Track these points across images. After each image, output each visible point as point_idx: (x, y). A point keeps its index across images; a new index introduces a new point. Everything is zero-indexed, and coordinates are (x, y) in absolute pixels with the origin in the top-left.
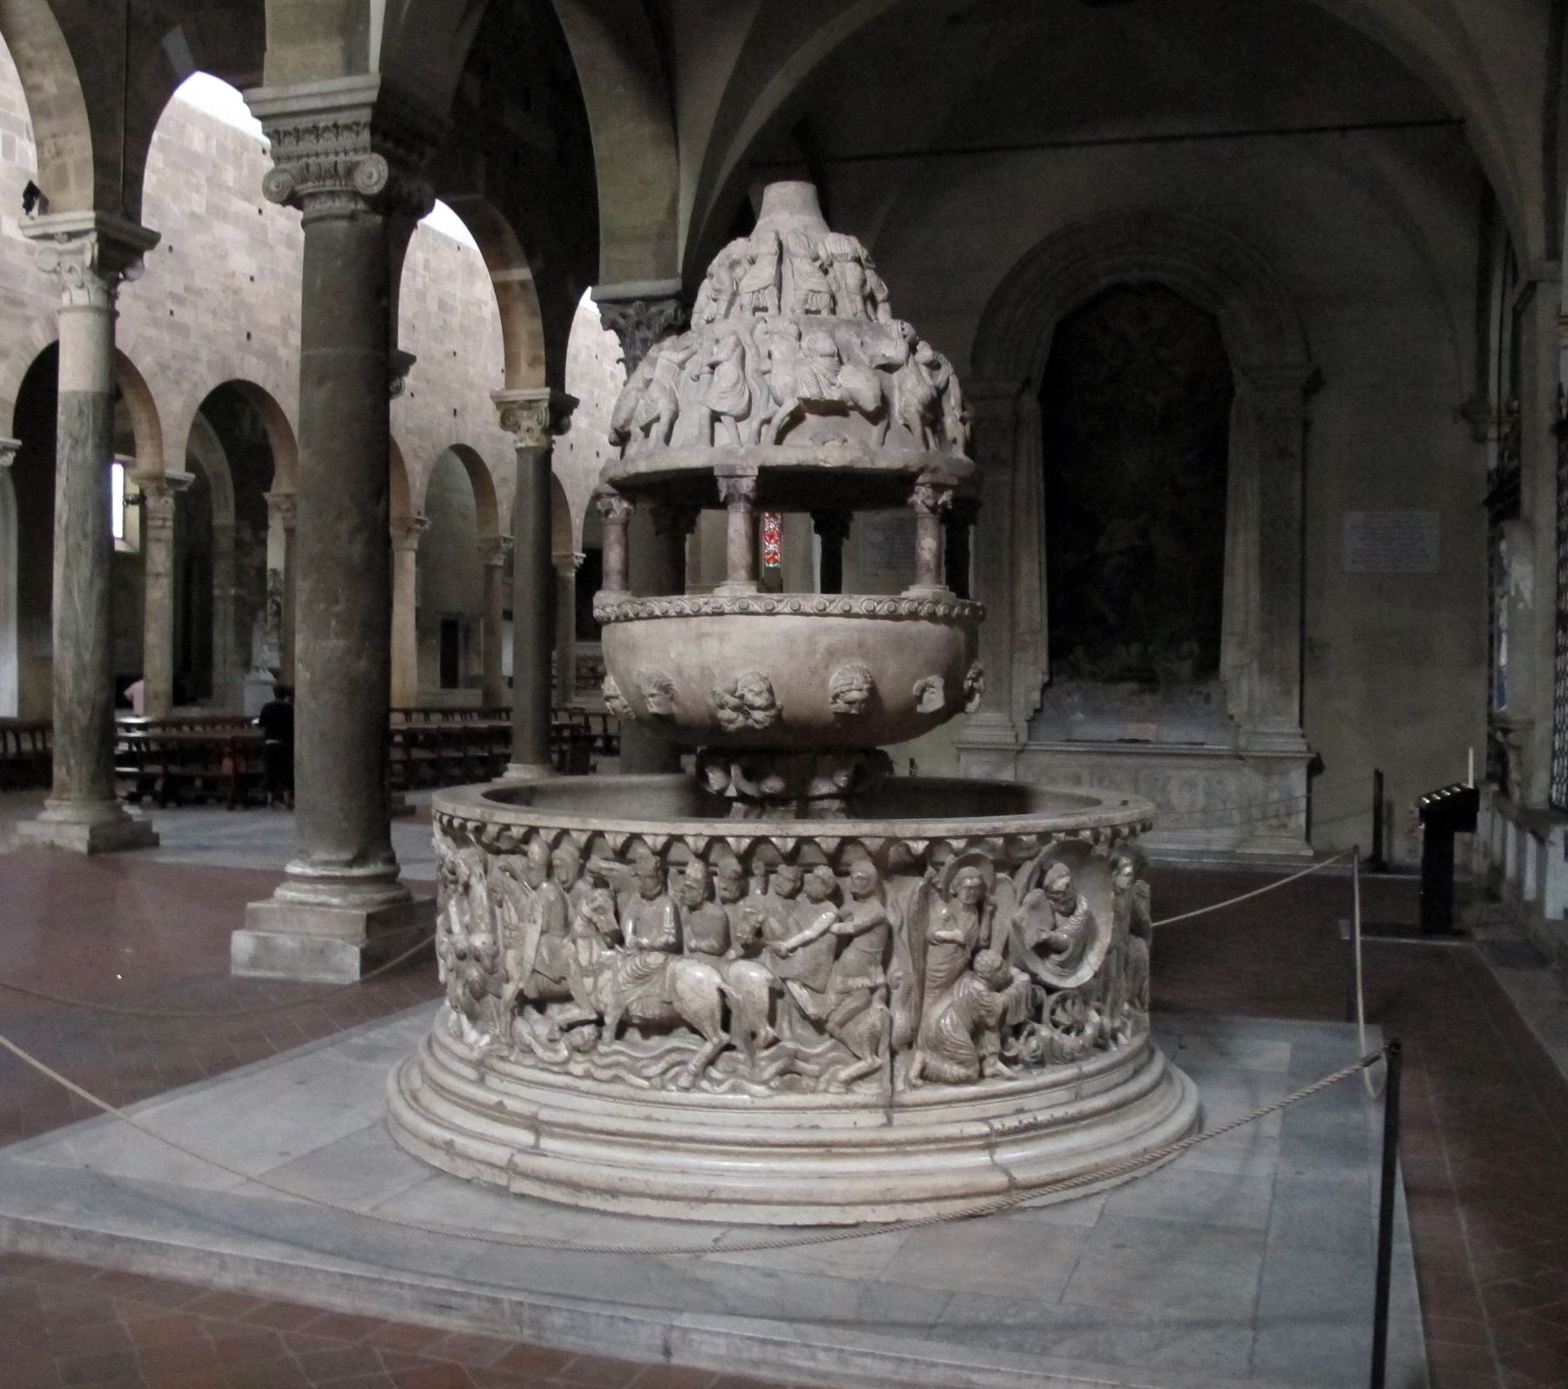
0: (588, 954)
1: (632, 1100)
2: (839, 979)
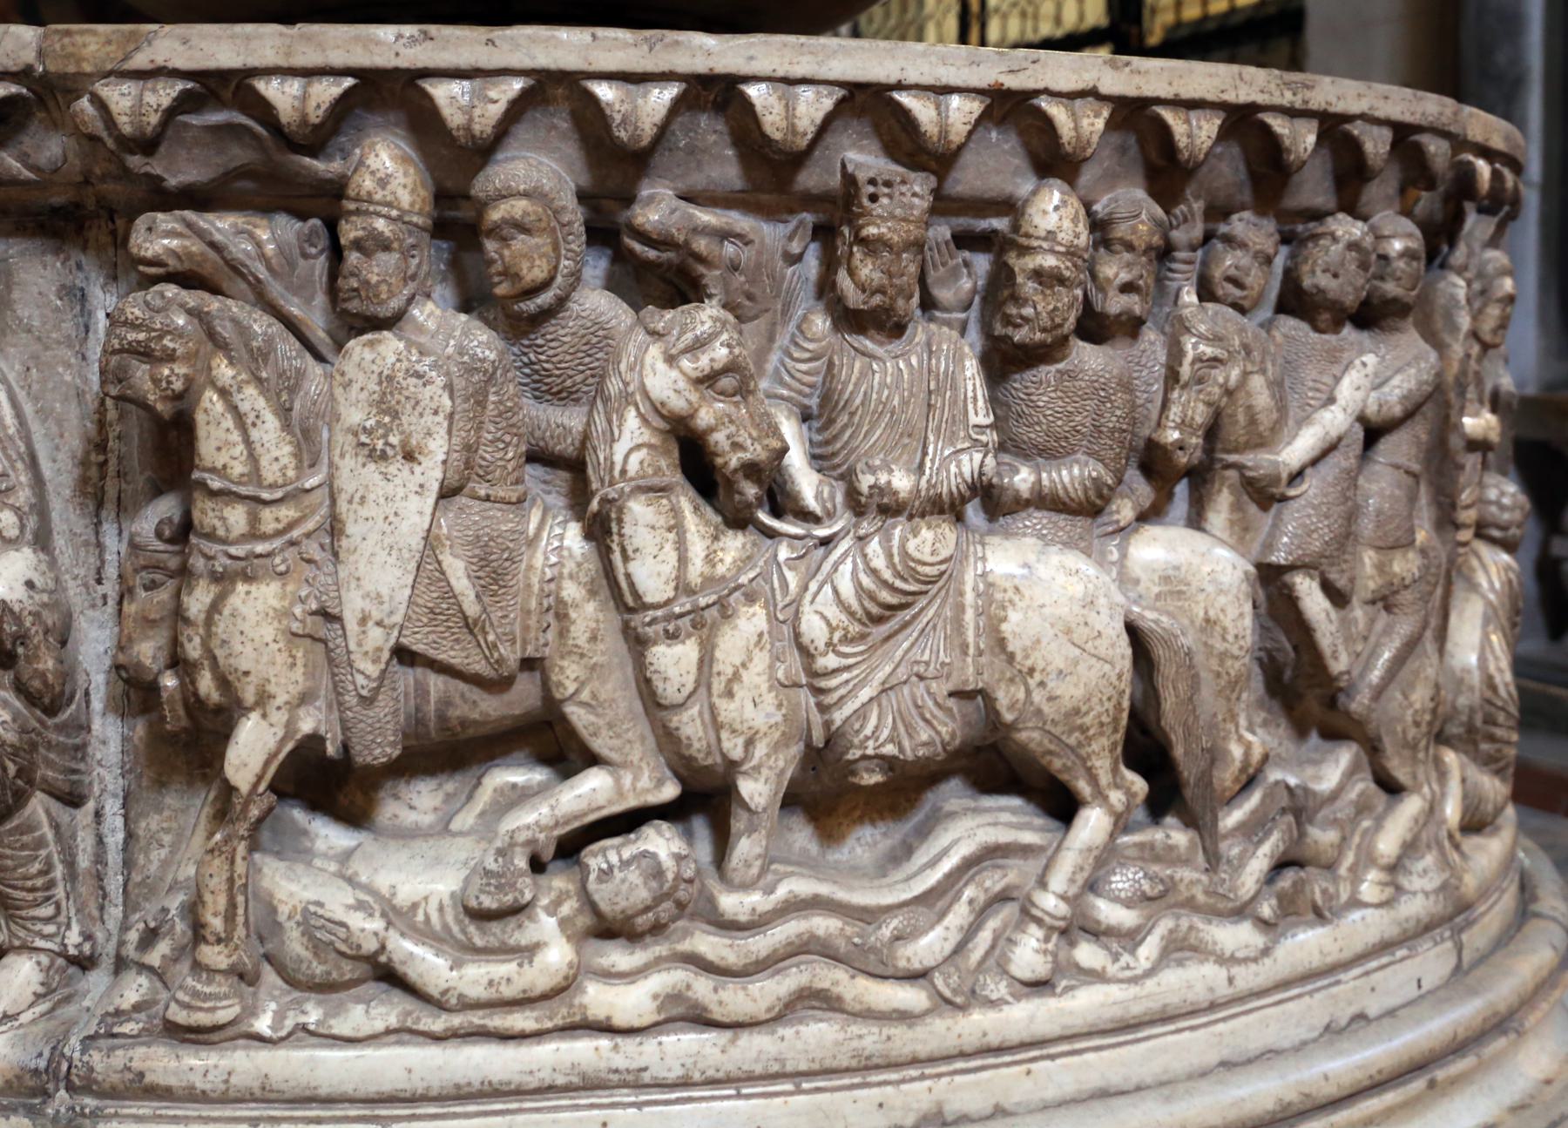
0: (671, 556)
1: (866, 1067)
2: (1369, 558)
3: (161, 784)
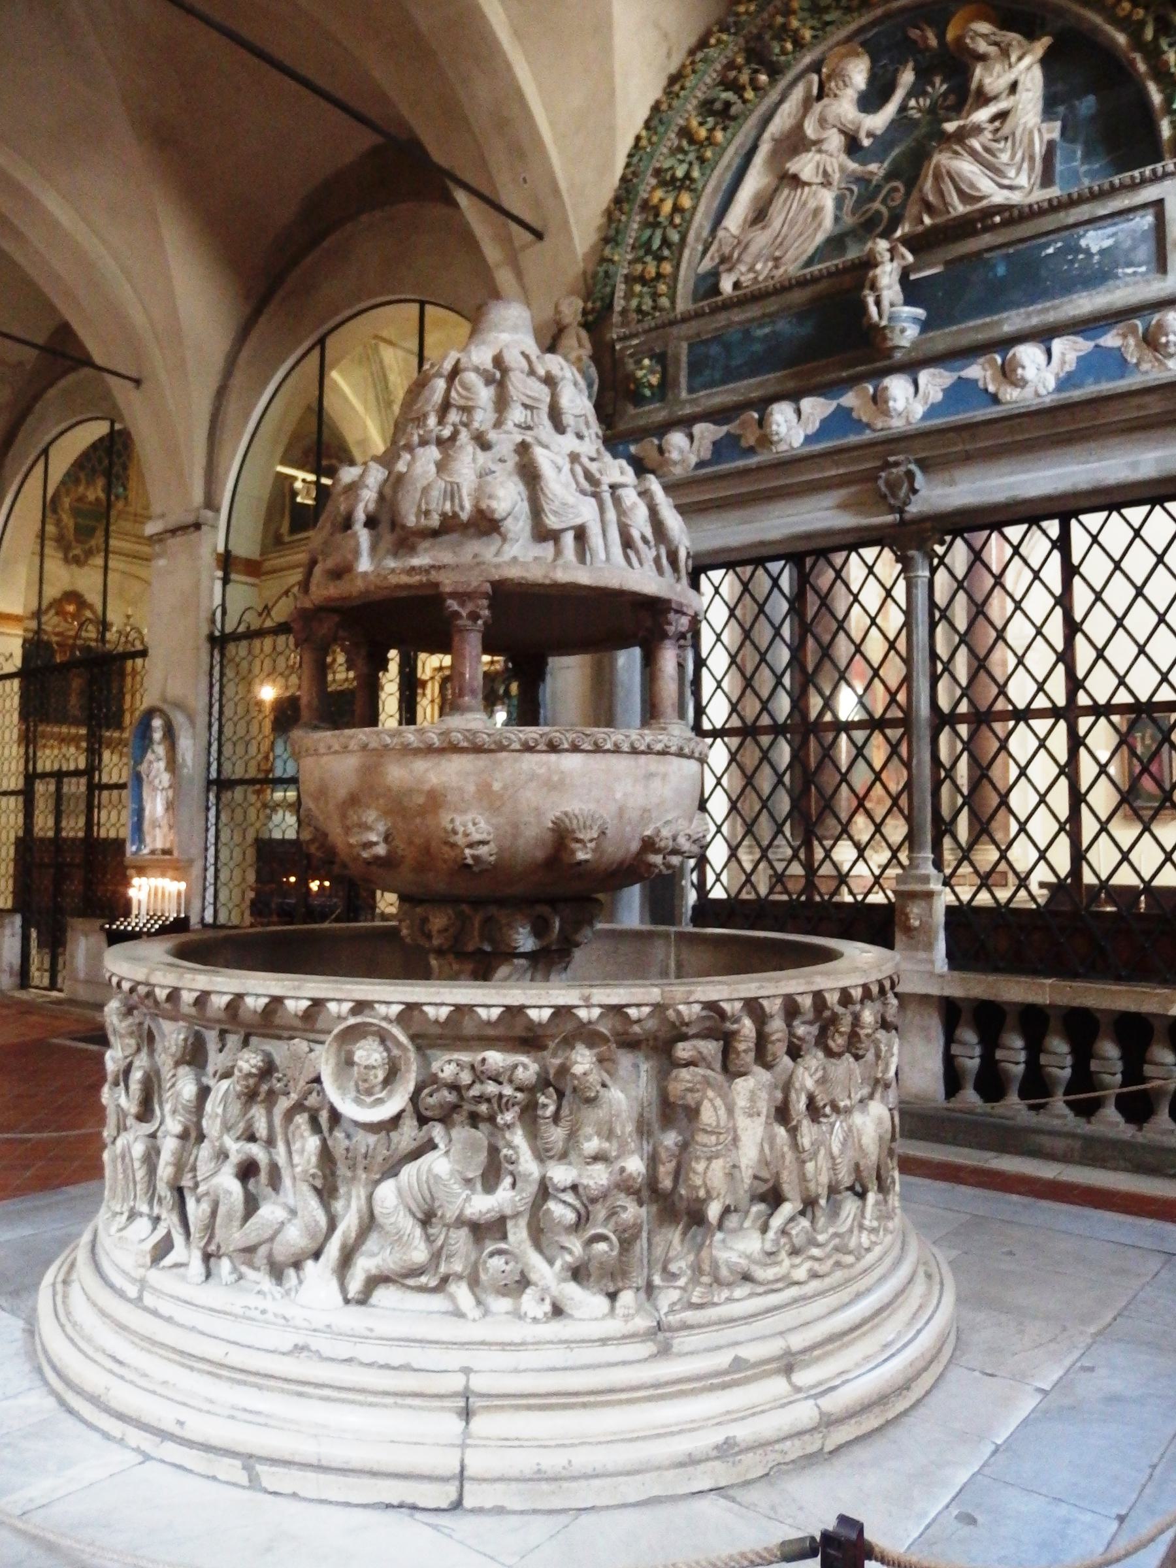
3: (661, 1225)
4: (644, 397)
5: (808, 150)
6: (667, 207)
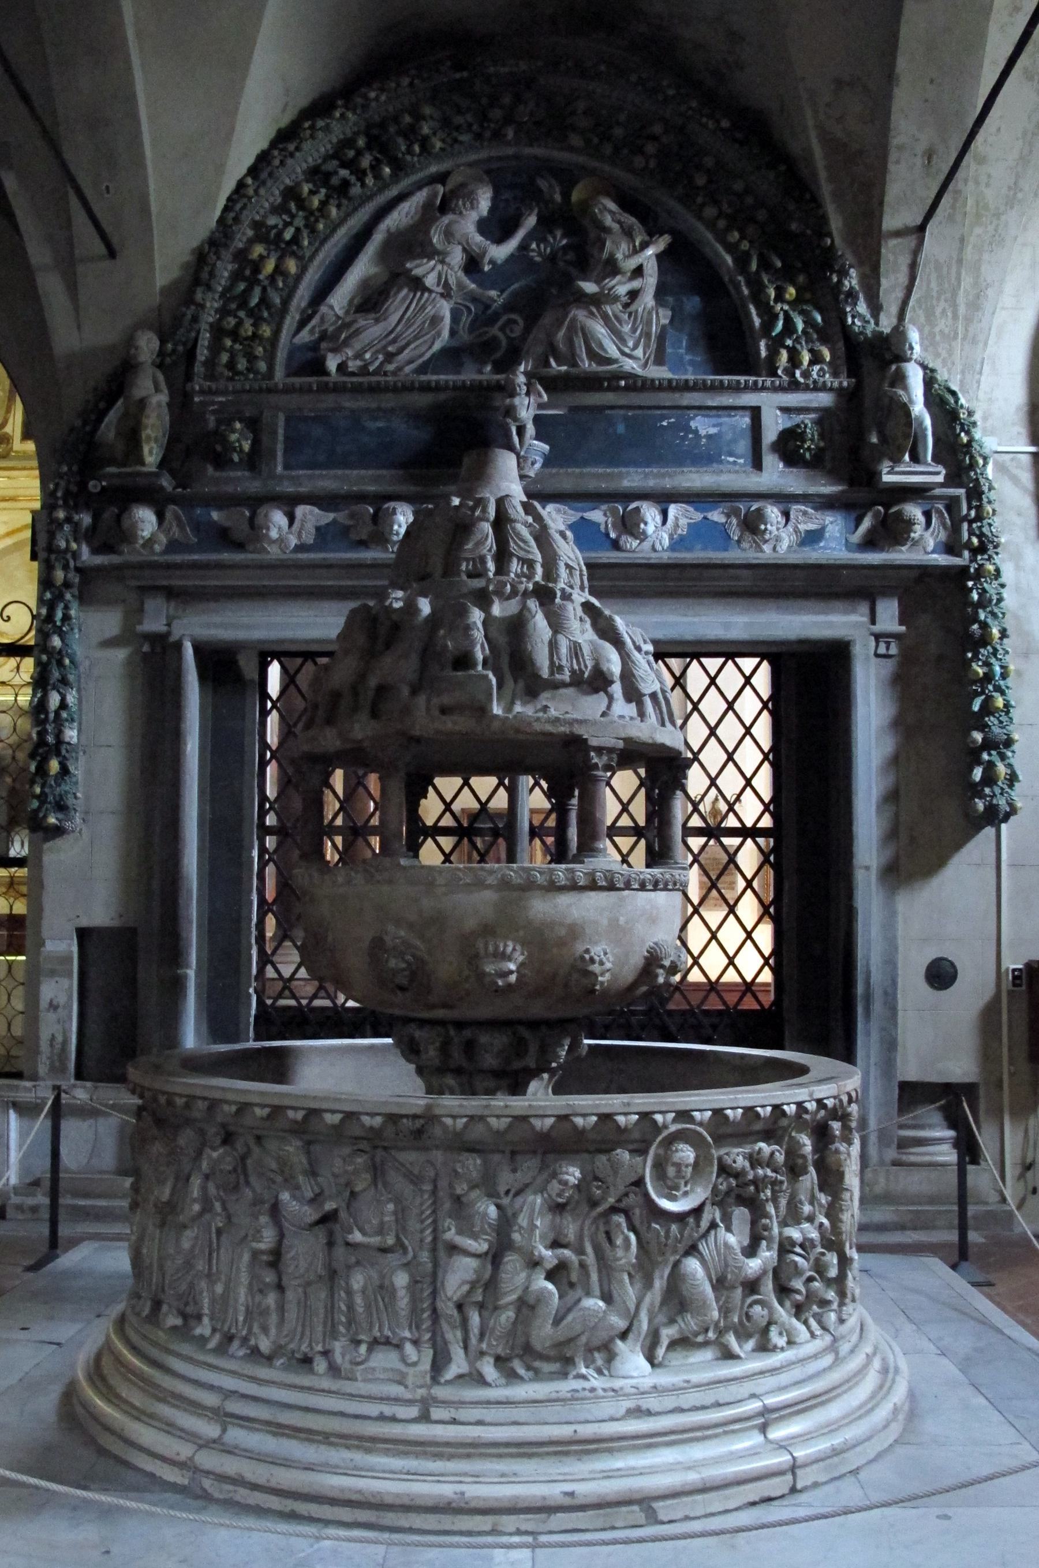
4: (232, 460)
5: (430, 258)
6: (270, 266)
